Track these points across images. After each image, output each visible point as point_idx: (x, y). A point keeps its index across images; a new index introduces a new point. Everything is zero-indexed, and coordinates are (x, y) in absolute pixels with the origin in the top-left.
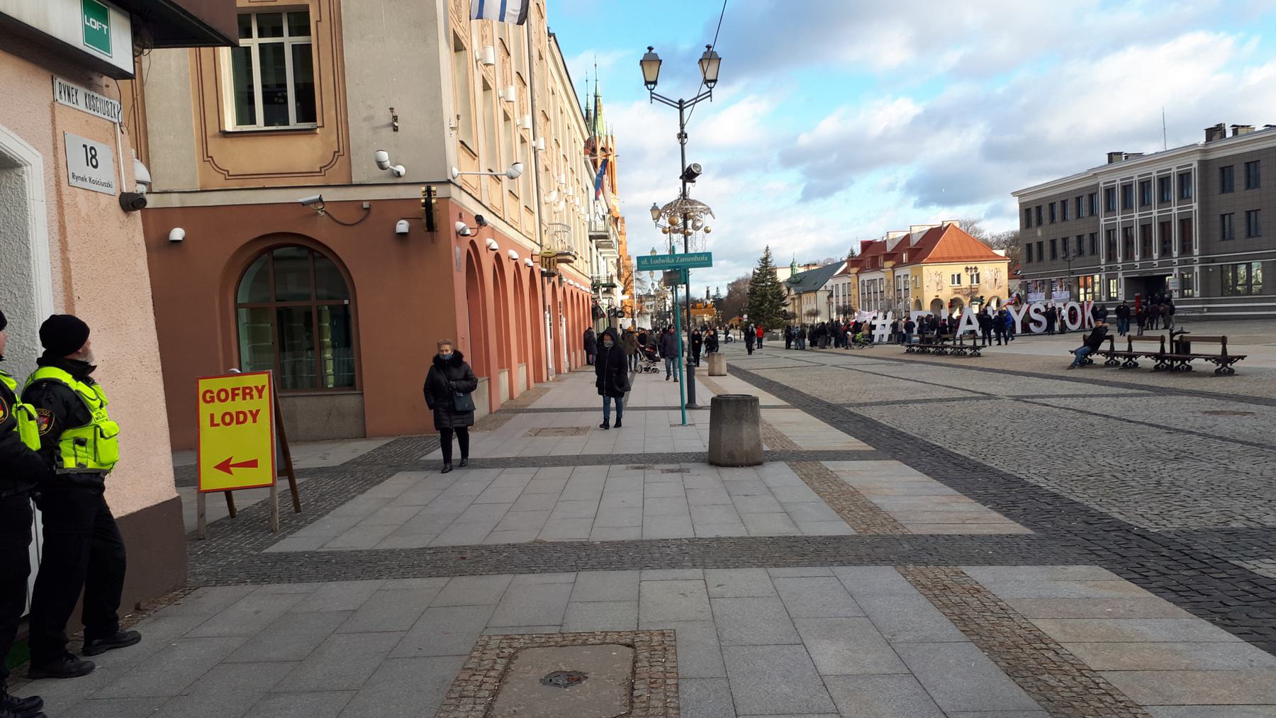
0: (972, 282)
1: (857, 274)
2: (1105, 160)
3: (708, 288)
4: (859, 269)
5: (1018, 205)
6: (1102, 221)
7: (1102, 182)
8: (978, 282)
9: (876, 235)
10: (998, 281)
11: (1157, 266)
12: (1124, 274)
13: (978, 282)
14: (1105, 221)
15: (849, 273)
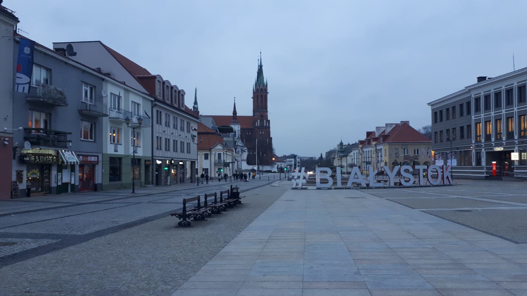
0: (415, 153)
1: (361, 148)
2: (476, 81)
3: (321, 154)
4: (362, 145)
5: (431, 110)
6: (473, 117)
7: (473, 95)
8: (418, 153)
9: (372, 129)
10: (429, 154)
11: (505, 145)
12: (485, 149)
13: (418, 153)
14: (475, 117)
15: (359, 148)
